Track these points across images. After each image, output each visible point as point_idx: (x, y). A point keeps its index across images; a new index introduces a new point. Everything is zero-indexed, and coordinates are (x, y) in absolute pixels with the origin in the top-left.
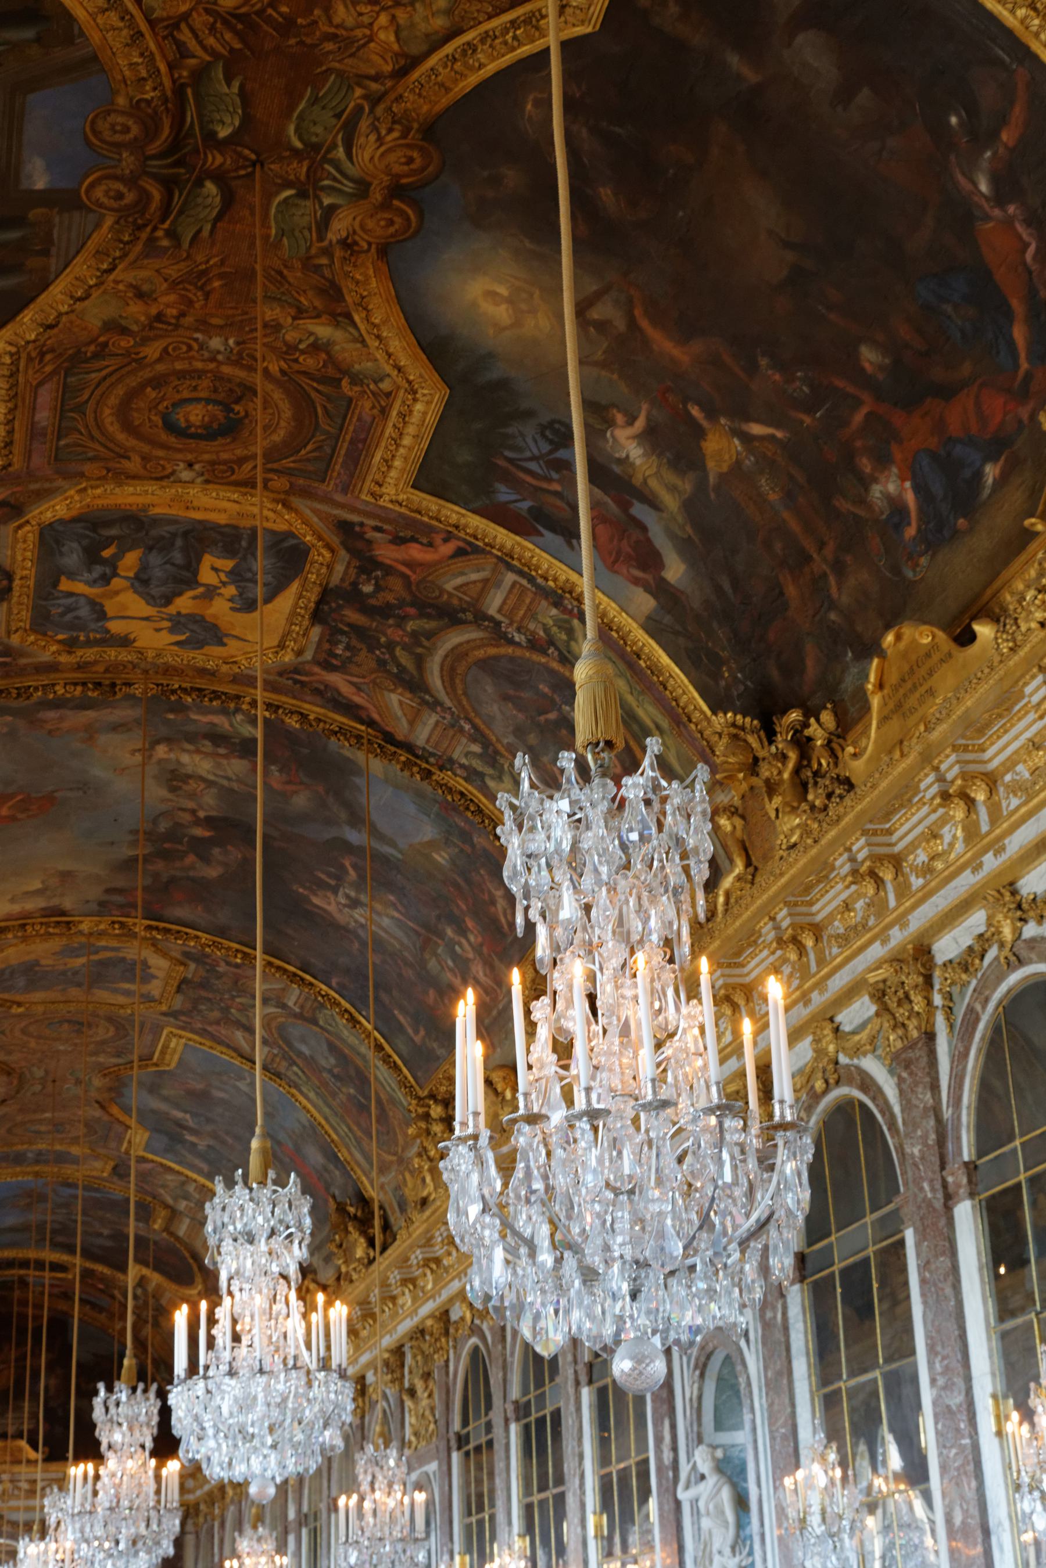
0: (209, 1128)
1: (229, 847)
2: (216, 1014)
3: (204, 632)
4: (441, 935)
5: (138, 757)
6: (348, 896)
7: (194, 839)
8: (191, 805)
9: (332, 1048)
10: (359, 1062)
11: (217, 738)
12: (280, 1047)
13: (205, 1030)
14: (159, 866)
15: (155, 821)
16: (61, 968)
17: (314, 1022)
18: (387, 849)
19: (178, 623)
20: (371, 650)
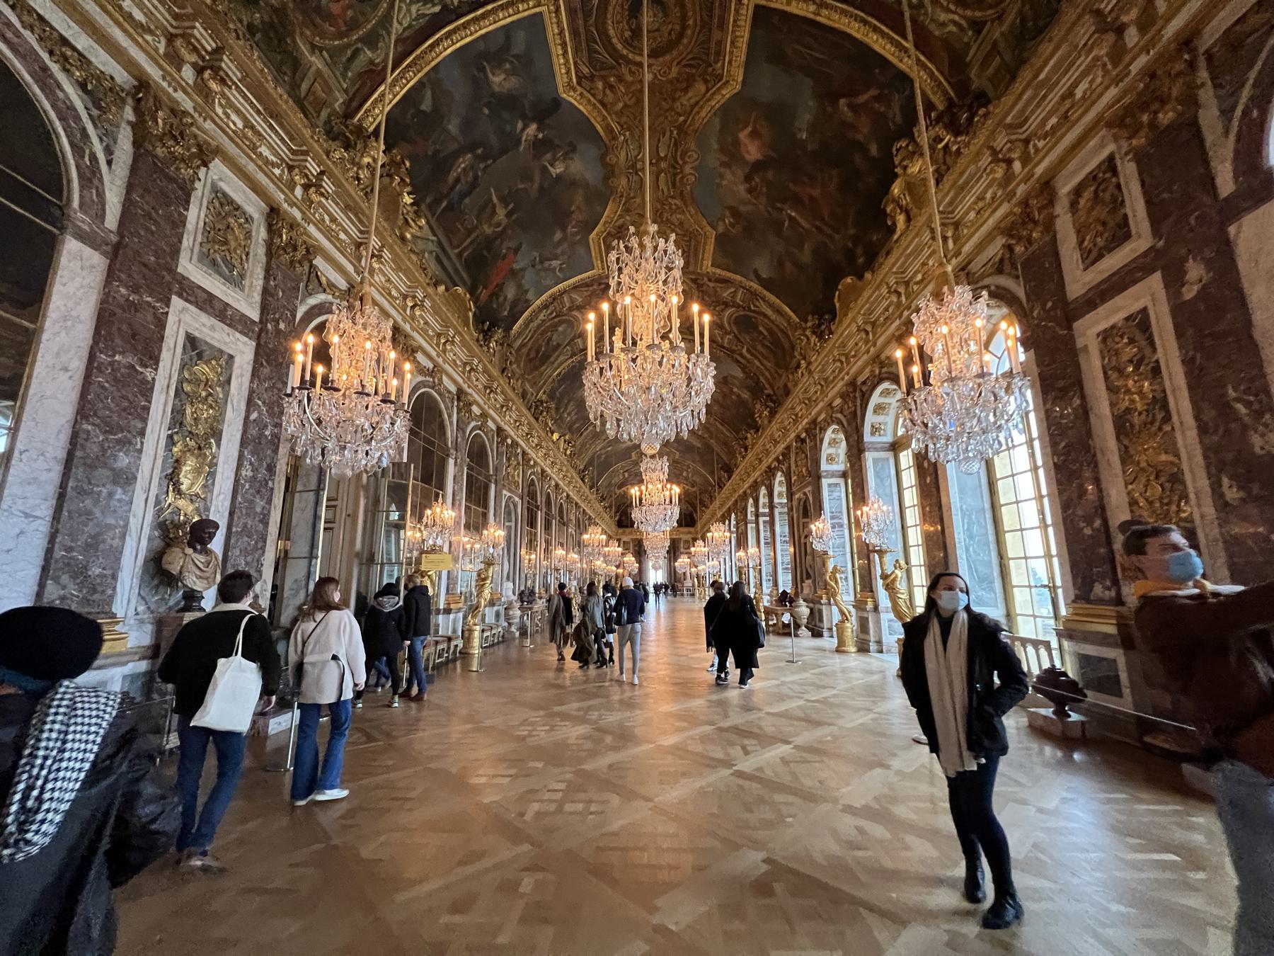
0: (537, 178)
9: (559, 345)
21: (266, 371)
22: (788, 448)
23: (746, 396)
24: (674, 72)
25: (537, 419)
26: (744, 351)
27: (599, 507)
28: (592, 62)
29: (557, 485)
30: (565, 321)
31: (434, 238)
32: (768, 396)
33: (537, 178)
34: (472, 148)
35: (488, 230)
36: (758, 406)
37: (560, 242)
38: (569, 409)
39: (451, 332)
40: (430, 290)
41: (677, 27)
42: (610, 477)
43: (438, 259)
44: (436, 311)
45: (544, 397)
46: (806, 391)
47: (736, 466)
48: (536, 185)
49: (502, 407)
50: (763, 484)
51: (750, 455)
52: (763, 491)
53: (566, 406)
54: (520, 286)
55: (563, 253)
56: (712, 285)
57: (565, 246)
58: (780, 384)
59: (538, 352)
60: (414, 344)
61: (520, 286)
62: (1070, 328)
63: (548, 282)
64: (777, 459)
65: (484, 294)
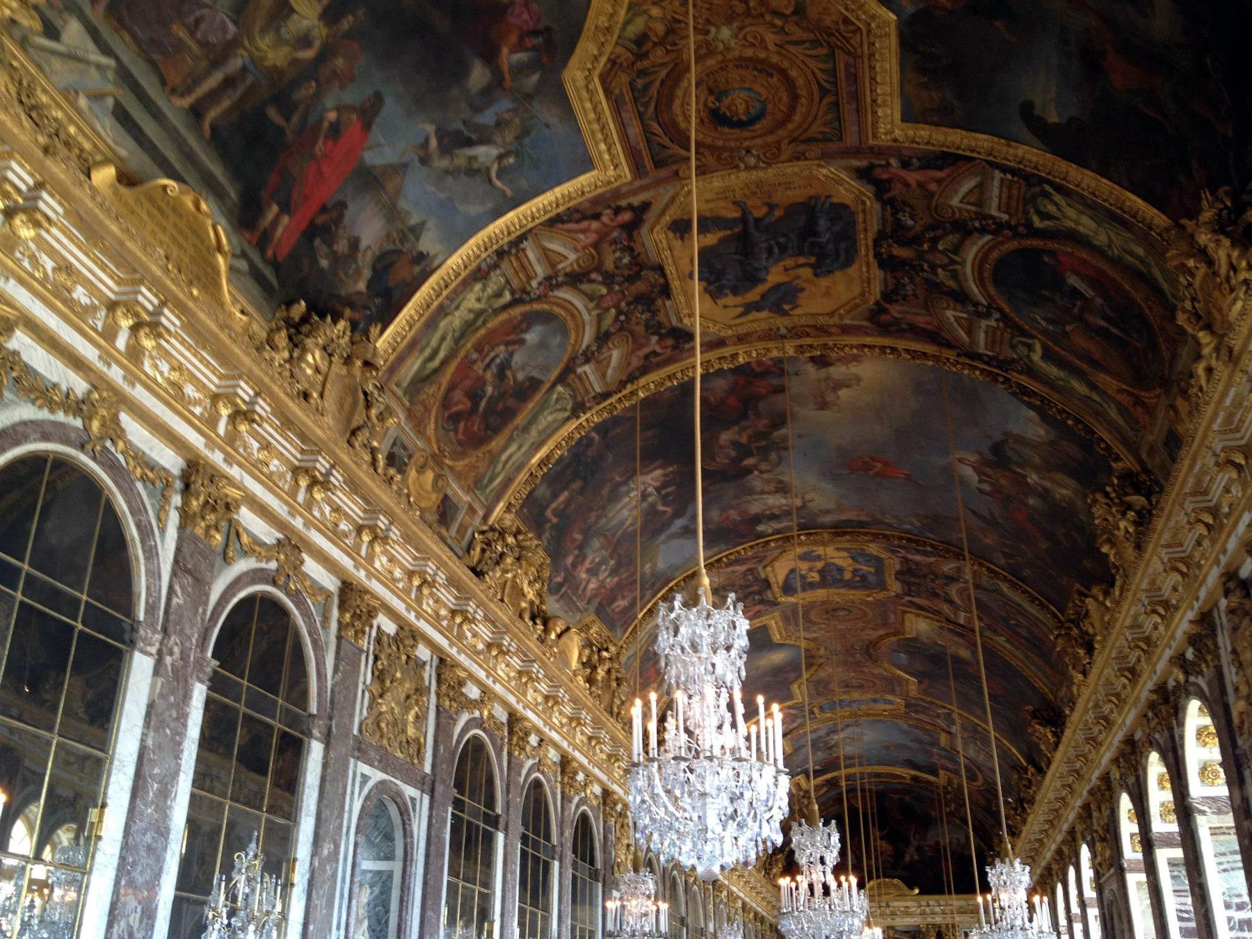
1: (727, 461)
2: (609, 265)
3: (804, 557)
4: (611, 557)
5: (808, 497)
6: (650, 495)
7: (751, 454)
8: (765, 476)
10: (520, 420)
11: (774, 517)
12: (539, 299)
13: (597, 217)
14: (762, 424)
15: (780, 460)
16: (789, 262)
17: (561, 379)
18: (663, 537)
19: (818, 558)
20: (741, 586)
22: (1206, 619)
25: (478, 573)
29: (565, 763)
30: (546, 318)
31: (104, 60)
32: (1127, 476)
36: (1098, 511)
37: (488, 94)
38: (592, 557)
39: (147, 298)
43: (122, 116)
44: (91, 233)
45: (509, 520)
47: (1072, 702)
49: (359, 530)
50: (1153, 744)
51: (1103, 667)
52: (1155, 767)
53: (582, 547)
54: (392, 213)
55: (500, 124)
56: (912, 177)
57: (503, 105)
58: (1155, 436)
59: (474, 396)
61: (392, 213)
63: (474, 209)
64: (1179, 660)
65: (284, 228)
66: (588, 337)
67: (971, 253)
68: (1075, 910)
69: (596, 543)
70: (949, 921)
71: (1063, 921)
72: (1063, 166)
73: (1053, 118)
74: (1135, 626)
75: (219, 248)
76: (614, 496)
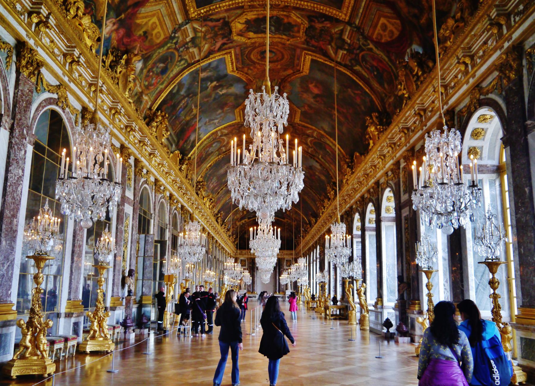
0: (213, 96)
9: (212, 152)
17: (217, 151)
21: (135, 216)
23: (323, 178)
24: (279, 67)
25: (197, 194)
26: (320, 157)
27: (225, 237)
28: (243, 63)
33: (213, 96)
34: (188, 96)
35: (188, 118)
38: (213, 181)
40: (168, 159)
41: (280, 57)
42: (233, 214)
46: (348, 191)
48: (212, 98)
49: (184, 194)
55: (221, 117)
56: (300, 127)
57: (222, 114)
59: (200, 158)
60: (161, 183)
62: (400, 212)
66: (225, 143)
67: (309, 139)
68: (315, 259)
69: (215, 178)
70: (282, 257)
71: (312, 261)
72: (327, 136)
73: (326, 130)
74: (332, 210)
75: (179, 157)
76: (221, 168)
